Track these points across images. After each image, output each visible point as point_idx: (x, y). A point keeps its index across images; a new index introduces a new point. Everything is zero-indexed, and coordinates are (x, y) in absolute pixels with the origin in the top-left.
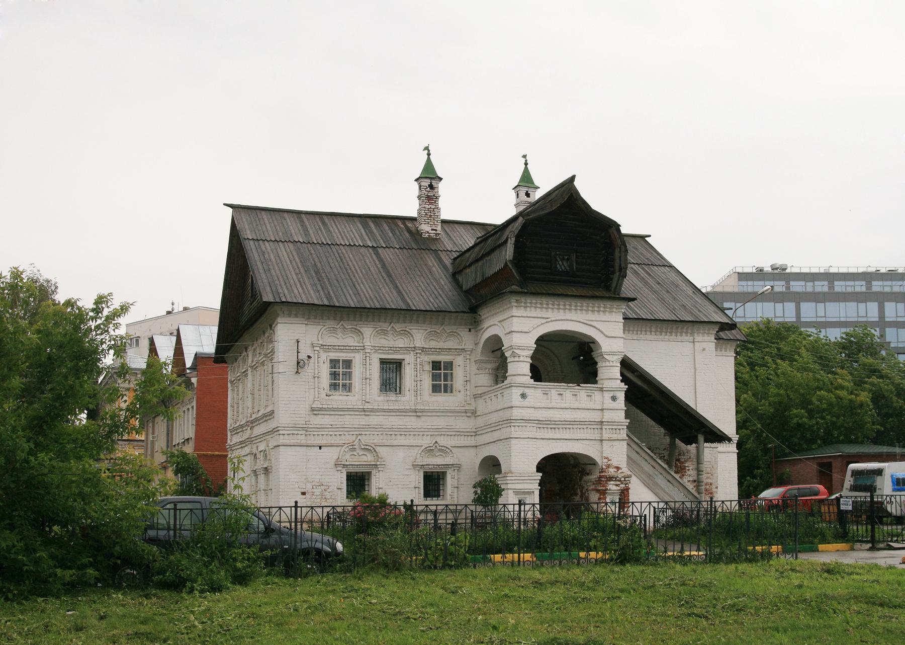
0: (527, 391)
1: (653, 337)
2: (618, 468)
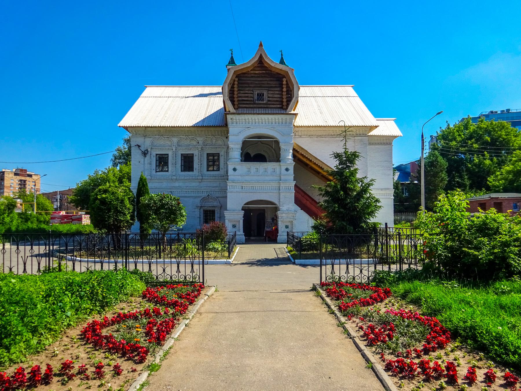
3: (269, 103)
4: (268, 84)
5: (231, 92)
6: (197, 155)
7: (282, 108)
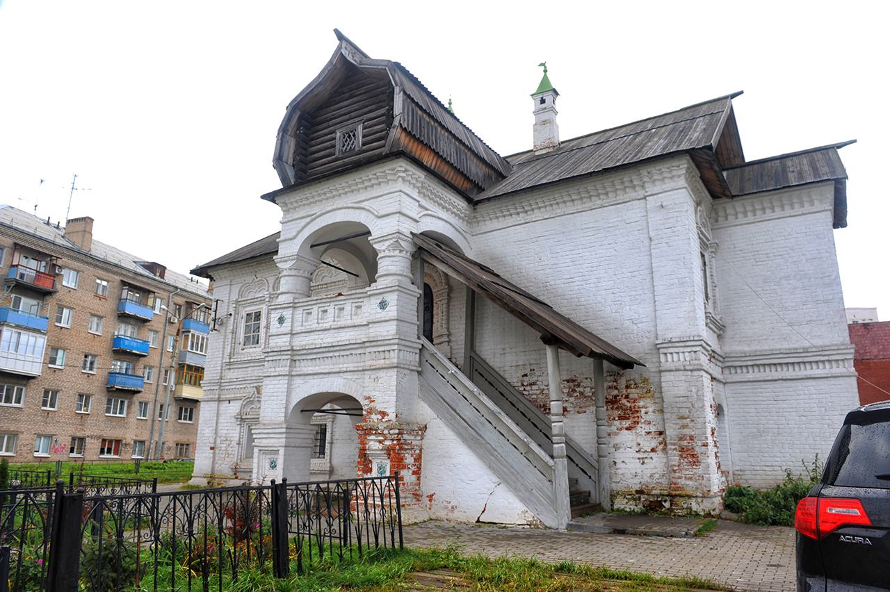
1: (578, 206)
2: (384, 414)
3: (364, 147)
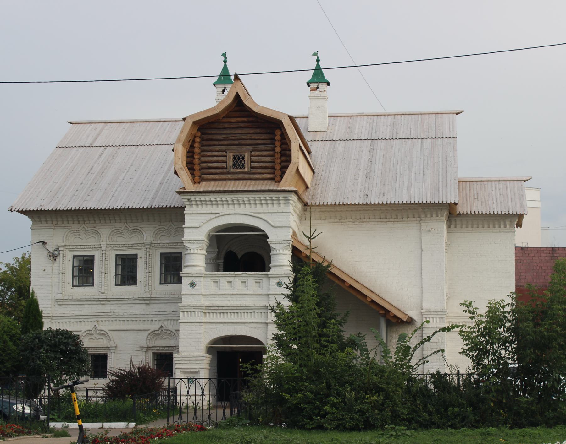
0: (196, 280)
3: (254, 171)
4: (251, 139)
5: (190, 154)
6: (143, 256)
7: (272, 179)
